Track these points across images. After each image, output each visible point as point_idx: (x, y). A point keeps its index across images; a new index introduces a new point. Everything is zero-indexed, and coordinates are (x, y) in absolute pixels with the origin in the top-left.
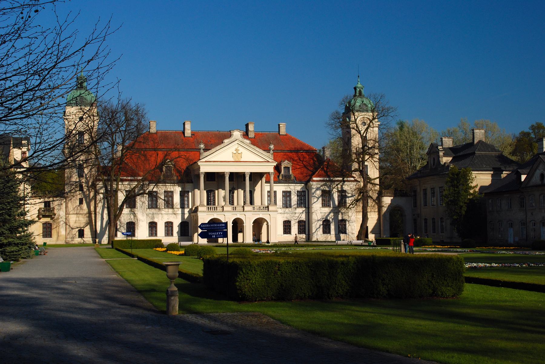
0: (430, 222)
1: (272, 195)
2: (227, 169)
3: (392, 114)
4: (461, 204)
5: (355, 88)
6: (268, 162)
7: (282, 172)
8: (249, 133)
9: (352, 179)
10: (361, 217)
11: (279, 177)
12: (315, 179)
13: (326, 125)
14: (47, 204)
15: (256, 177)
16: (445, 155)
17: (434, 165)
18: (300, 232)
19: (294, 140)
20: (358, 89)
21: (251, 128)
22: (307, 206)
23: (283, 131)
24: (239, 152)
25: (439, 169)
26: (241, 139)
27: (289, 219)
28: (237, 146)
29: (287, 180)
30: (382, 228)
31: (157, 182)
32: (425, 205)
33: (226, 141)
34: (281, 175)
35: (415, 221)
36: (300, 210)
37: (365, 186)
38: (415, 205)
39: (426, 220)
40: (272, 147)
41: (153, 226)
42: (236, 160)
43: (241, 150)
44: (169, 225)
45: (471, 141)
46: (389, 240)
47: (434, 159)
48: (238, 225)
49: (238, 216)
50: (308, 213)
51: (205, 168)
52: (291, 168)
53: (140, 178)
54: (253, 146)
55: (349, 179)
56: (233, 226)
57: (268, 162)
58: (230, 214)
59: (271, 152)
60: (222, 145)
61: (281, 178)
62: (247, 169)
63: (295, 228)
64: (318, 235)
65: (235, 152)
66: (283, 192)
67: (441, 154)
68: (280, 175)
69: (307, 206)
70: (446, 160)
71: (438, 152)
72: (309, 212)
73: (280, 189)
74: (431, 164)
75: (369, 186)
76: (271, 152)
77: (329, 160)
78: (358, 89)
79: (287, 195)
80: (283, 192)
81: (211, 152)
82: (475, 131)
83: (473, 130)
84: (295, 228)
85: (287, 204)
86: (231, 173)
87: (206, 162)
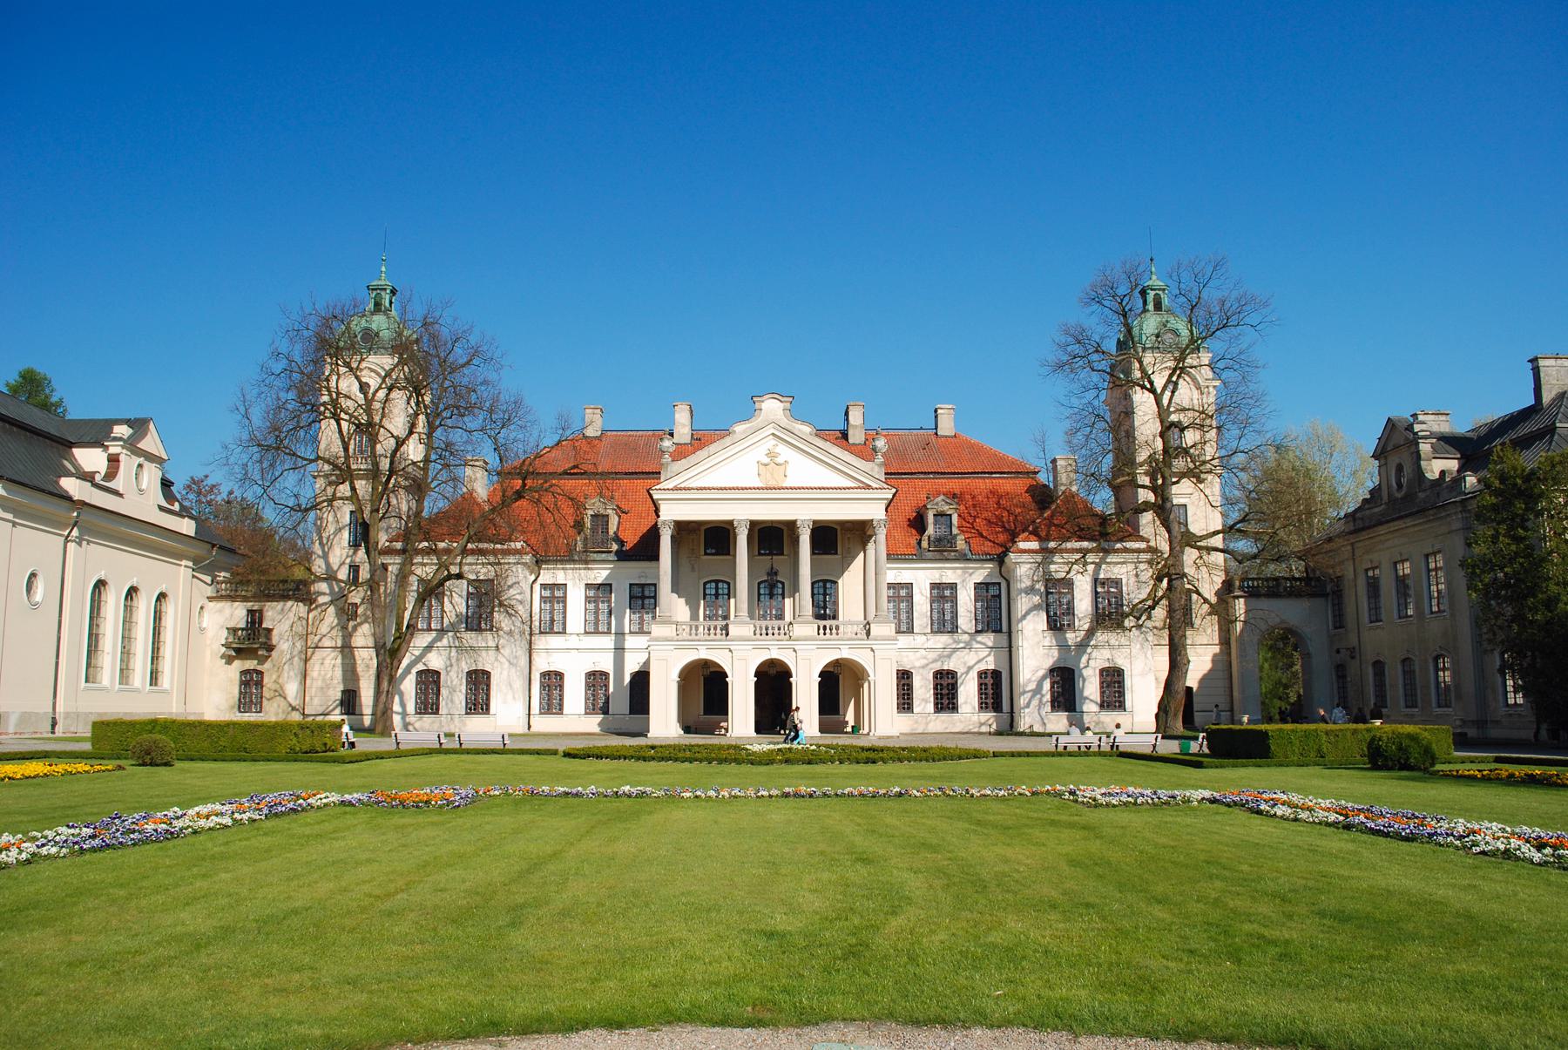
0: (1394, 675)
1: (902, 594)
2: (741, 513)
3: (1253, 319)
4: (1554, 588)
5: (1143, 293)
6: (869, 487)
7: (930, 530)
8: (850, 433)
9: (1143, 545)
10: (1167, 658)
11: (919, 543)
12: (1022, 545)
13: (1044, 371)
14: (255, 618)
15: (835, 540)
16: (1437, 454)
17: (1400, 486)
18: (983, 706)
19: (976, 450)
20: (1152, 293)
21: (856, 417)
22: (1005, 628)
23: (947, 426)
24: (779, 460)
25: (1421, 495)
26: (785, 422)
28: (772, 442)
29: (943, 550)
30: (1236, 694)
31: (567, 557)
32: (1376, 617)
33: (739, 428)
34: (925, 537)
35: (1340, 671)
36: (988, 639)
37: (1176, 553)
38: (1339, 622)
39: (1379, 666)
40: (881, 443)
41: (553, 681)
42: (772, 483)
43: (785, 453)
44: (596, 679)
45: (1531, 401)
46: (1265, 734)
47: (1400, 468)
49: (775, 654)
50: (1009, 650)
51: (671, 512)
52: (955, 518)
53: (519, 545)
54: (820, 443)
55: (1130, 545)
56: (756, 683)
57: (869, 487)
58: (748, 646)
59: (880, 459)
60: (728, 440)
61: (925, 544)
62: (805, 513)
63: (968, 692)
64: (1036, 714)
65: (767, 460)
66: (934, 586)
67: (1425, 447)
68: (917, 532)
69: (1005, 628)
70: (1437, 466)
71: (1414, 440)
72: (1010, 647)
73: (922, 577)
74: (1389, 487)
75: (1190, 555)
76: (880, 459)
77: (1070, 497)
78: (1152, 293)
79: (943, 594)
80: (934, 586)
81: (692, 459)
82: (1541, 363)
83: (1534, 361)
84: (968, 692)
85: (944, 623)
86: (753, 524)
87: (676, 489)
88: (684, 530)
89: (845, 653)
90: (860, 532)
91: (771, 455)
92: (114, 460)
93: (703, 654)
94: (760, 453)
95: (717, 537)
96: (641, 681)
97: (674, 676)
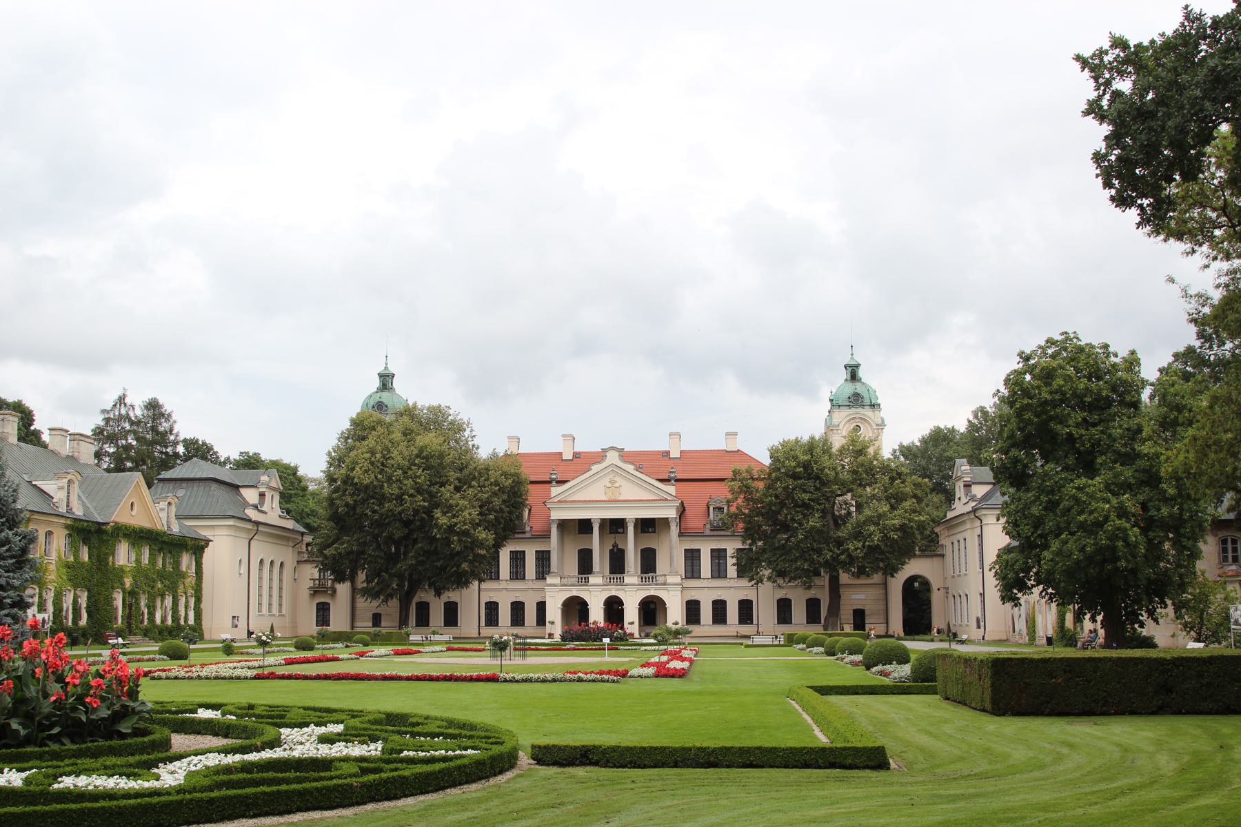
2: (596, 515)
27: (723, 598)
41: (492, 608)
43: (620, 481)
48: (614, 608)
49: (614, 593)
62: (630, 515)
79: (718, 555)
85: (719, 572)
88: (563, 525)
89: (652, 593)
90: (665, 522)
91: (612, 482)
92: (262, 495)
93: (575, 593)
94: (606, 482)
95: (584, 526)
96: (541, 607)
97: (560, 606)
